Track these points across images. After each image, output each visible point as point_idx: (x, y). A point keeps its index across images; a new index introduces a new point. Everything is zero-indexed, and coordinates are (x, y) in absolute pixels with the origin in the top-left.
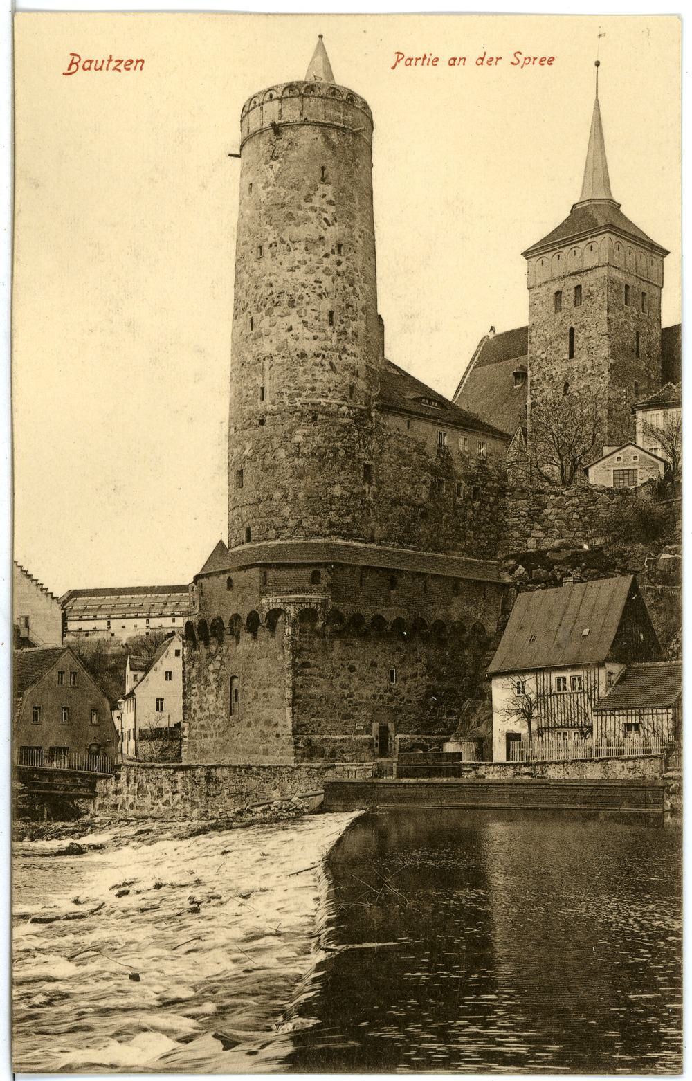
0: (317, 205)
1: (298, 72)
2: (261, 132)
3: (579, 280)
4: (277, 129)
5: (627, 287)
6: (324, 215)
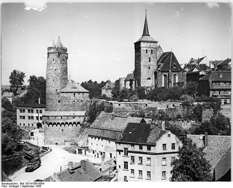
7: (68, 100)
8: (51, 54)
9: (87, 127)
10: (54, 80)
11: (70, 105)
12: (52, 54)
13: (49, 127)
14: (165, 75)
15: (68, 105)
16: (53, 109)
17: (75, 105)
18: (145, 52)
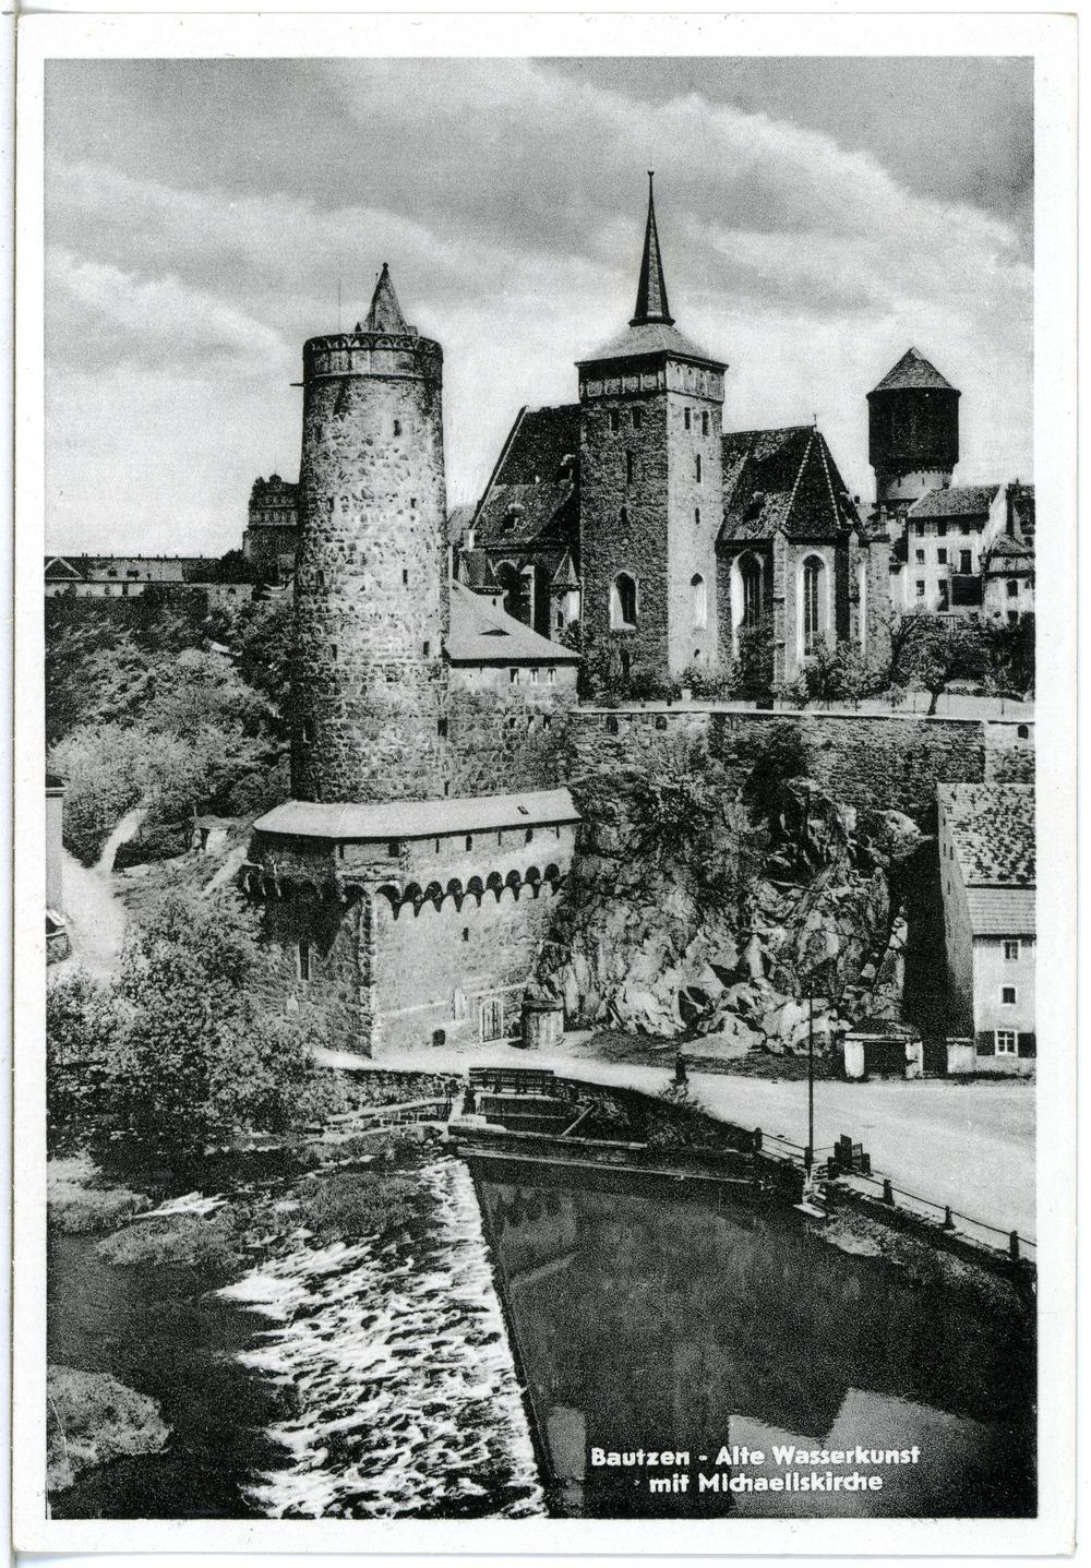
0: (390, 461)
6: (397, 471)
7: (482, 715)
8: (370, 384)
9: (625, 893)
10: (405, 572)
11: (493, 749)
12: (383, 387)
13: (396, 917)
14: (813, 565)
15: (483, 750)
16: (406, 787)
17: (518, 746)
18: (682, 420)
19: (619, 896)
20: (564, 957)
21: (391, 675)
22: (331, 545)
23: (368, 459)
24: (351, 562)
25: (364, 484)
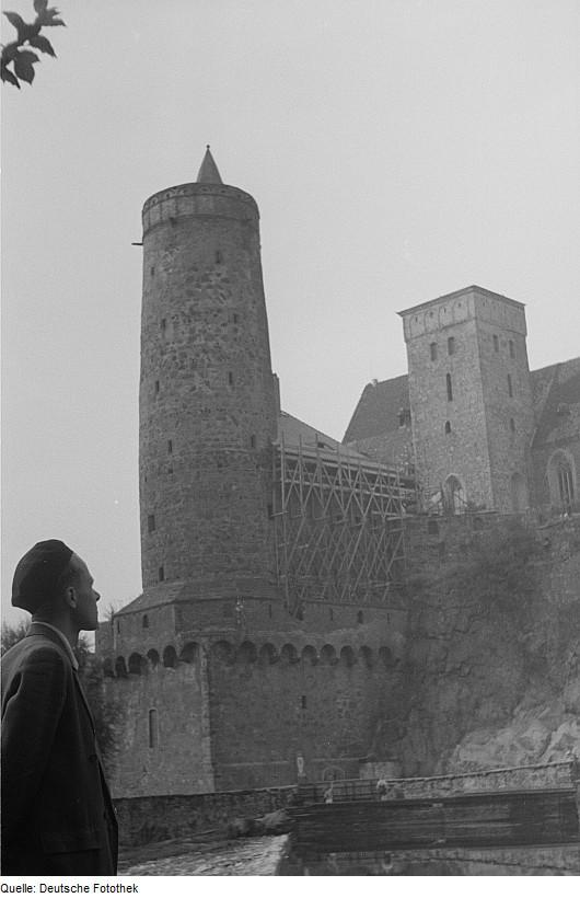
0: (213, 283)
1: (191, 176)
2: (161, 223)
3: (451, 333)
4: (173, 221)
5: (495, 337)
16: (240, 560)
19: (454, 671)
20: (401, 731)
21: (222, 461)
22: (165, 357)
23: (195, 283)
24: (182, 368)
25: (192, 302)
